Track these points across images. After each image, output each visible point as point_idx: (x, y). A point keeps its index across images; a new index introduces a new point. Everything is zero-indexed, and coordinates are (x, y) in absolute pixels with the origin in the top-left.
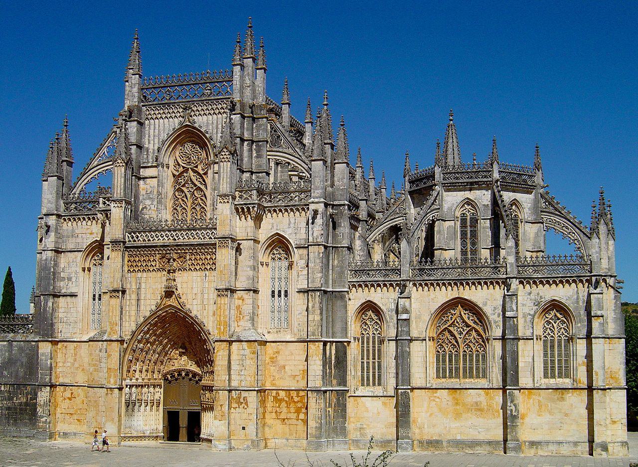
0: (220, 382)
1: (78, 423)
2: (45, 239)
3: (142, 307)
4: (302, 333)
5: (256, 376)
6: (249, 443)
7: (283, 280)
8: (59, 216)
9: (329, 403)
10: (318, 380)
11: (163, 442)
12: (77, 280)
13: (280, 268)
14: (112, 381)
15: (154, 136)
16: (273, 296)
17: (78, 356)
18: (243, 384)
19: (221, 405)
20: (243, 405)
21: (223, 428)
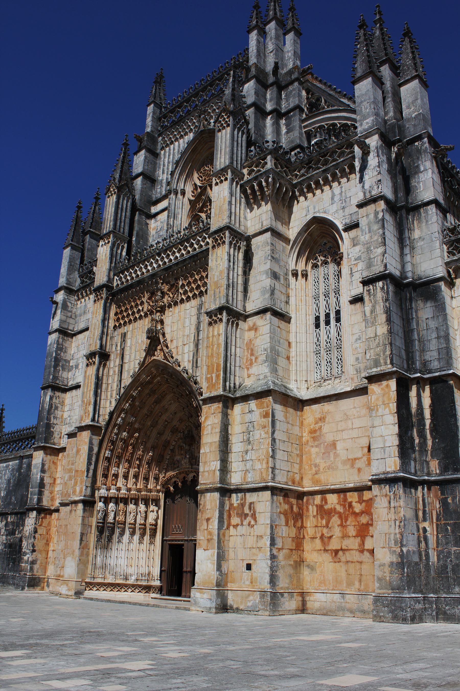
0: (206, 474)
5: (270, 459)
6: (258, 600)
7: (332, 295)
9: (424, 512)
11: (158, 596)
13: (326, 278)
14: (78, 489)
15: (169, 162)
16: (317, 326)
20: (249, 518)
21: (210, 565)
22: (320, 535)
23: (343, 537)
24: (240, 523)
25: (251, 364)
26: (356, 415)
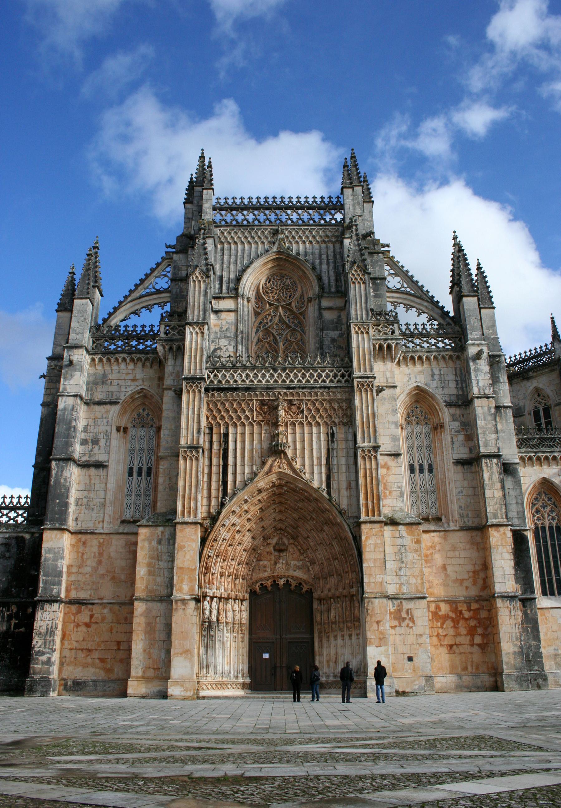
0: (373, 585)
1: (101, 665)
2: (65, 378)
3: (230, 477)
4: (466, 520)
6: (424, 683)
8: (87, 351)
10: (509, 581)
12: (108, 444)
14: (185, 587)
17: (105, 555)
18: (405, 589)
19: (378, 622)
20: (407, 622)
22: (436, 634)
23: (455, 636)
24: (397, 624)
25: (385, 496)
26: (462, 548)
